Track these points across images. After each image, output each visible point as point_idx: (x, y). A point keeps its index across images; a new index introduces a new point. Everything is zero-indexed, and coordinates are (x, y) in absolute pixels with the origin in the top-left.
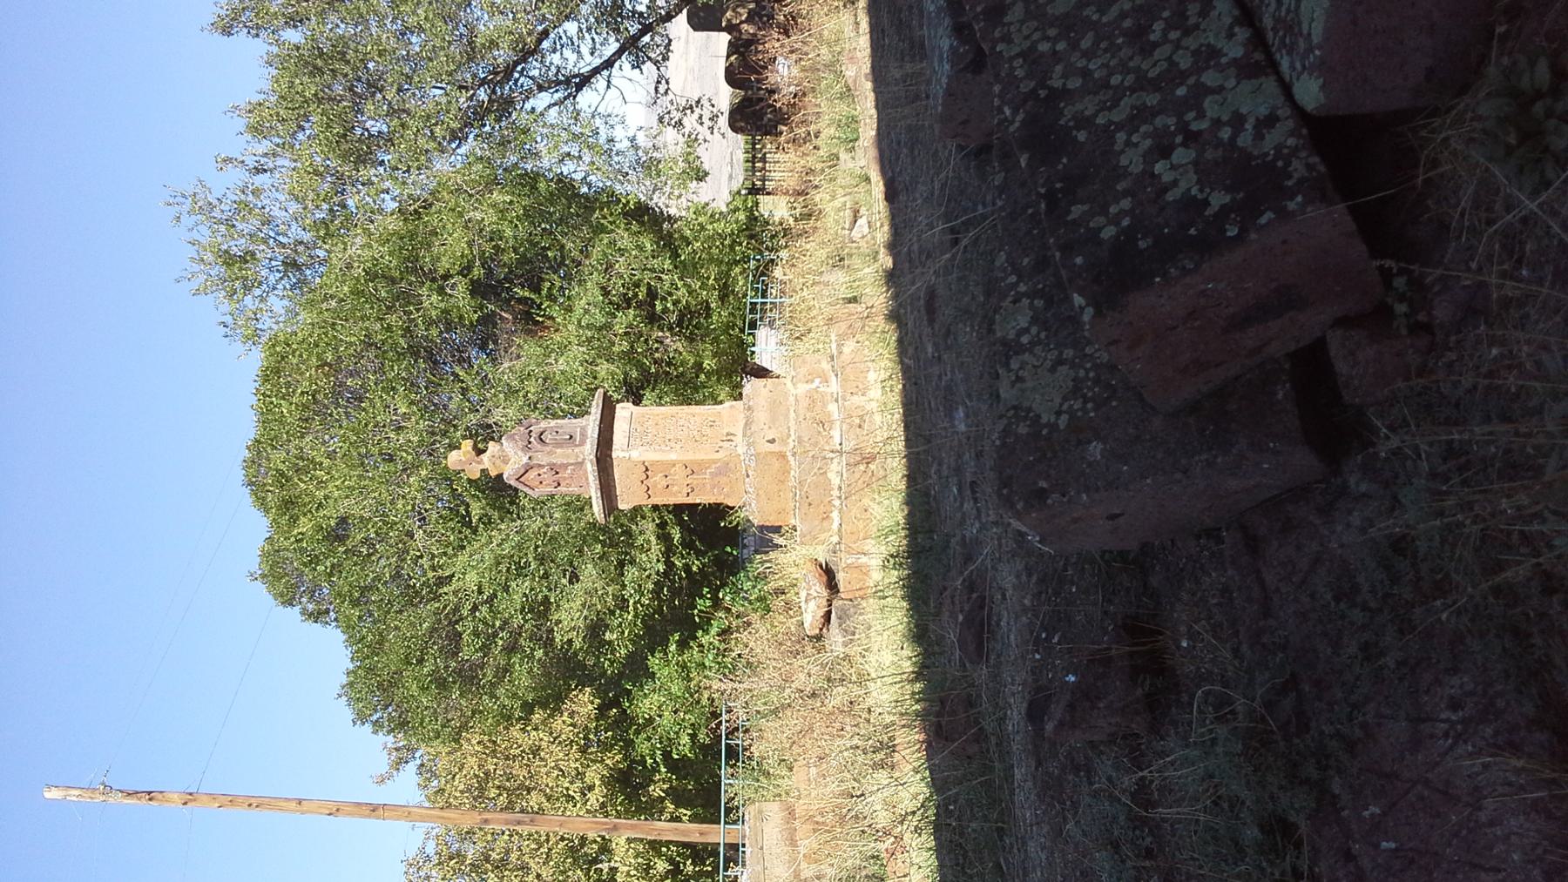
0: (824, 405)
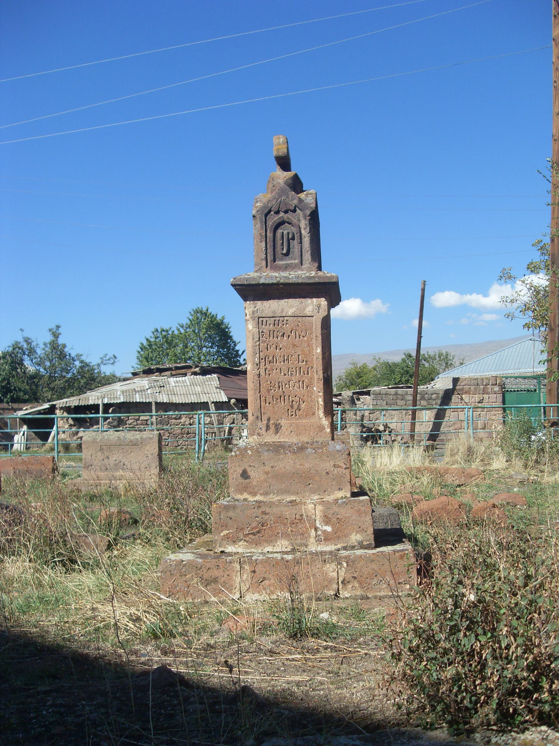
0: (285, 535)
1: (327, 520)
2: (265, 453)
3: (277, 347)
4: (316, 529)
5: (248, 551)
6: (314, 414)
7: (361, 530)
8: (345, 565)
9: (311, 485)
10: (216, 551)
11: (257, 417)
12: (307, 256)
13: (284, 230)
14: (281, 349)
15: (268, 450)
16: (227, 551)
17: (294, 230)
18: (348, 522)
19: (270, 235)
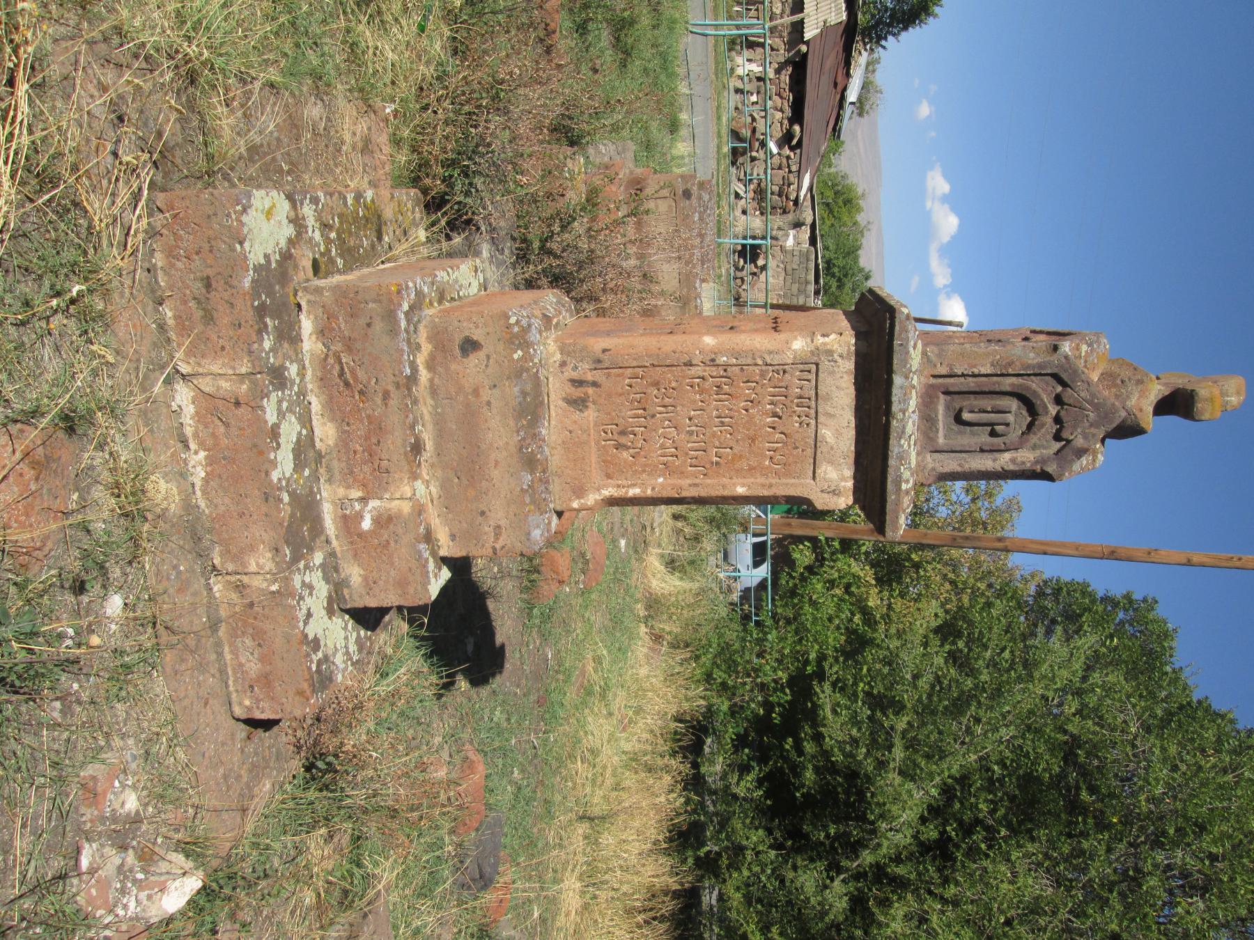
0: (344, 439)
1: (383, 521)
2: (516, 389)
3: (752, 402)
4: (364, 500)
5: (307, 363)
6: (609, 476)
7: (369, 584)
8: (274, 588)
9: (457, 480)
10: (300, 294)
11: (599, 361)
12: (951, 464)
13: (1015, 414)
14: (747, 410)
15: (524, 394)
16: (303, 317)
17: (1014, 434)
18: (384, 562)
19: (1008, 383)
